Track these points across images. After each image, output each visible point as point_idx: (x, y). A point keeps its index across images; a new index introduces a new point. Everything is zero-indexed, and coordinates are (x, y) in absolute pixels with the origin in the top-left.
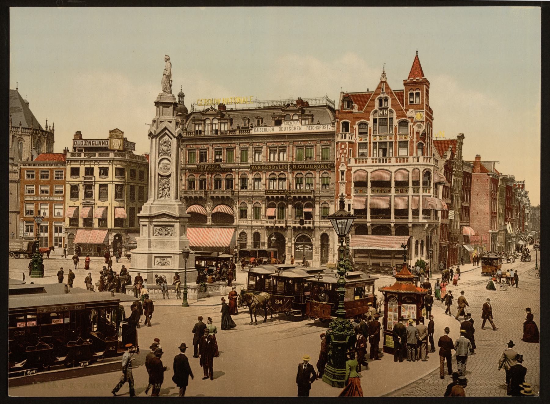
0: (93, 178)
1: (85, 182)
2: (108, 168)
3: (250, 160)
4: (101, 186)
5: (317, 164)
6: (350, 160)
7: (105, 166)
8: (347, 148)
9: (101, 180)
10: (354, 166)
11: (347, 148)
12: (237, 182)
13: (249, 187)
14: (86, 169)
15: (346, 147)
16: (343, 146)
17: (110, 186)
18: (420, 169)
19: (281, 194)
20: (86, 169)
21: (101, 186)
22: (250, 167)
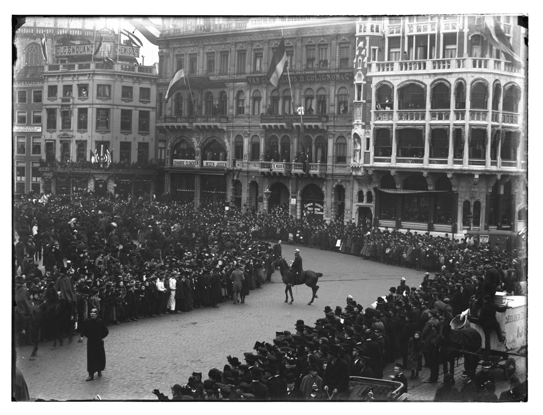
0: (71, 100)
1: (62, 106)
2: (88, 84)
3: (248, 69)
4: (80, 110)
5: (331, 74)
6: (370, 66)
7: (84, 82)
8: (367, 47)
9: (80, 102)
10: (376, 76)
11: (367, 47)
12: (231, 104)
13: (246, 111)
14: (65, 86)
15: (365, 44)
16: (361, 44)
17: (90, 111)
18: (466, 79)
19: (280, 122)
20: (65, 86)
21: (80, 110)
22: (246, 80)
